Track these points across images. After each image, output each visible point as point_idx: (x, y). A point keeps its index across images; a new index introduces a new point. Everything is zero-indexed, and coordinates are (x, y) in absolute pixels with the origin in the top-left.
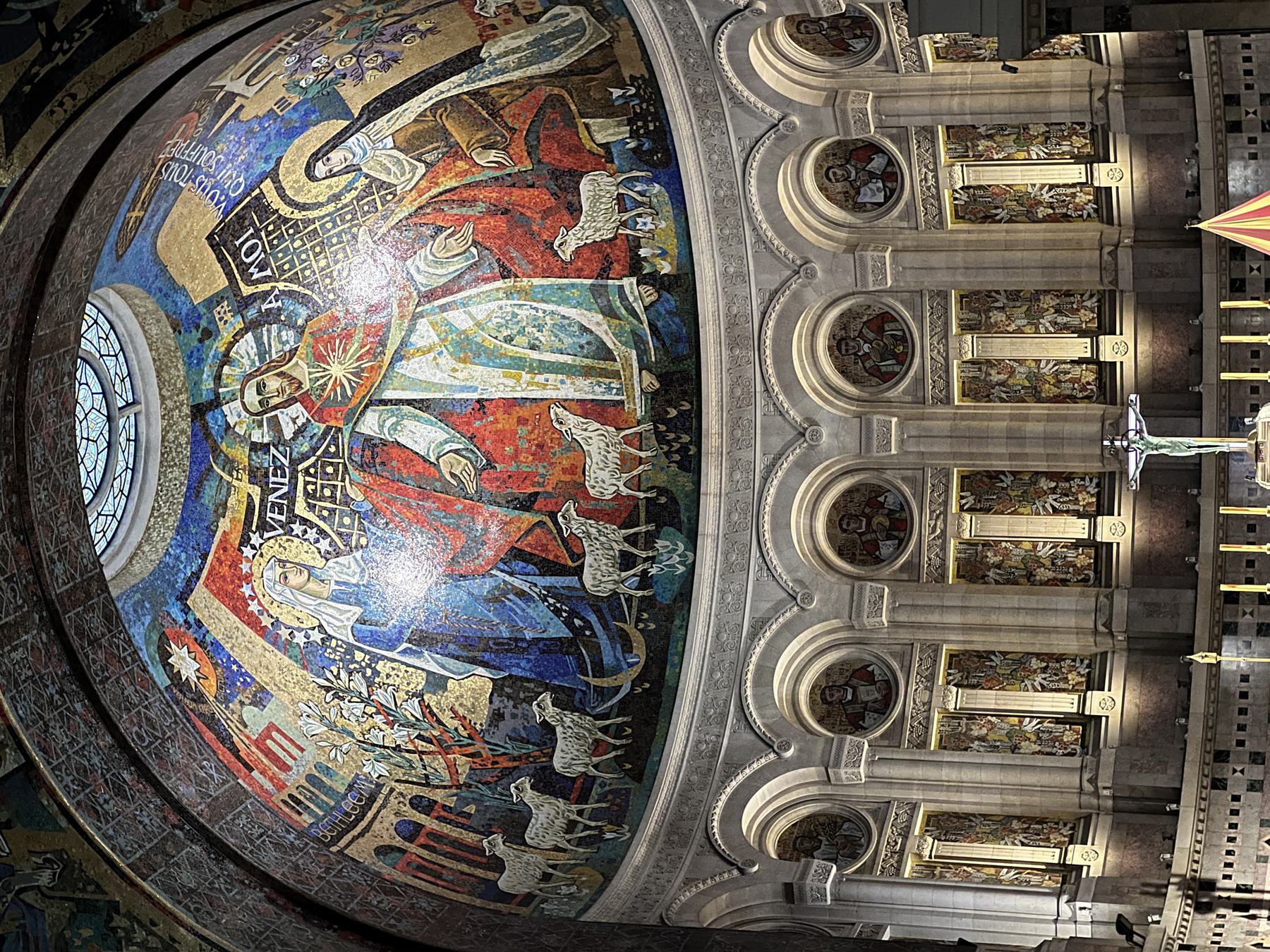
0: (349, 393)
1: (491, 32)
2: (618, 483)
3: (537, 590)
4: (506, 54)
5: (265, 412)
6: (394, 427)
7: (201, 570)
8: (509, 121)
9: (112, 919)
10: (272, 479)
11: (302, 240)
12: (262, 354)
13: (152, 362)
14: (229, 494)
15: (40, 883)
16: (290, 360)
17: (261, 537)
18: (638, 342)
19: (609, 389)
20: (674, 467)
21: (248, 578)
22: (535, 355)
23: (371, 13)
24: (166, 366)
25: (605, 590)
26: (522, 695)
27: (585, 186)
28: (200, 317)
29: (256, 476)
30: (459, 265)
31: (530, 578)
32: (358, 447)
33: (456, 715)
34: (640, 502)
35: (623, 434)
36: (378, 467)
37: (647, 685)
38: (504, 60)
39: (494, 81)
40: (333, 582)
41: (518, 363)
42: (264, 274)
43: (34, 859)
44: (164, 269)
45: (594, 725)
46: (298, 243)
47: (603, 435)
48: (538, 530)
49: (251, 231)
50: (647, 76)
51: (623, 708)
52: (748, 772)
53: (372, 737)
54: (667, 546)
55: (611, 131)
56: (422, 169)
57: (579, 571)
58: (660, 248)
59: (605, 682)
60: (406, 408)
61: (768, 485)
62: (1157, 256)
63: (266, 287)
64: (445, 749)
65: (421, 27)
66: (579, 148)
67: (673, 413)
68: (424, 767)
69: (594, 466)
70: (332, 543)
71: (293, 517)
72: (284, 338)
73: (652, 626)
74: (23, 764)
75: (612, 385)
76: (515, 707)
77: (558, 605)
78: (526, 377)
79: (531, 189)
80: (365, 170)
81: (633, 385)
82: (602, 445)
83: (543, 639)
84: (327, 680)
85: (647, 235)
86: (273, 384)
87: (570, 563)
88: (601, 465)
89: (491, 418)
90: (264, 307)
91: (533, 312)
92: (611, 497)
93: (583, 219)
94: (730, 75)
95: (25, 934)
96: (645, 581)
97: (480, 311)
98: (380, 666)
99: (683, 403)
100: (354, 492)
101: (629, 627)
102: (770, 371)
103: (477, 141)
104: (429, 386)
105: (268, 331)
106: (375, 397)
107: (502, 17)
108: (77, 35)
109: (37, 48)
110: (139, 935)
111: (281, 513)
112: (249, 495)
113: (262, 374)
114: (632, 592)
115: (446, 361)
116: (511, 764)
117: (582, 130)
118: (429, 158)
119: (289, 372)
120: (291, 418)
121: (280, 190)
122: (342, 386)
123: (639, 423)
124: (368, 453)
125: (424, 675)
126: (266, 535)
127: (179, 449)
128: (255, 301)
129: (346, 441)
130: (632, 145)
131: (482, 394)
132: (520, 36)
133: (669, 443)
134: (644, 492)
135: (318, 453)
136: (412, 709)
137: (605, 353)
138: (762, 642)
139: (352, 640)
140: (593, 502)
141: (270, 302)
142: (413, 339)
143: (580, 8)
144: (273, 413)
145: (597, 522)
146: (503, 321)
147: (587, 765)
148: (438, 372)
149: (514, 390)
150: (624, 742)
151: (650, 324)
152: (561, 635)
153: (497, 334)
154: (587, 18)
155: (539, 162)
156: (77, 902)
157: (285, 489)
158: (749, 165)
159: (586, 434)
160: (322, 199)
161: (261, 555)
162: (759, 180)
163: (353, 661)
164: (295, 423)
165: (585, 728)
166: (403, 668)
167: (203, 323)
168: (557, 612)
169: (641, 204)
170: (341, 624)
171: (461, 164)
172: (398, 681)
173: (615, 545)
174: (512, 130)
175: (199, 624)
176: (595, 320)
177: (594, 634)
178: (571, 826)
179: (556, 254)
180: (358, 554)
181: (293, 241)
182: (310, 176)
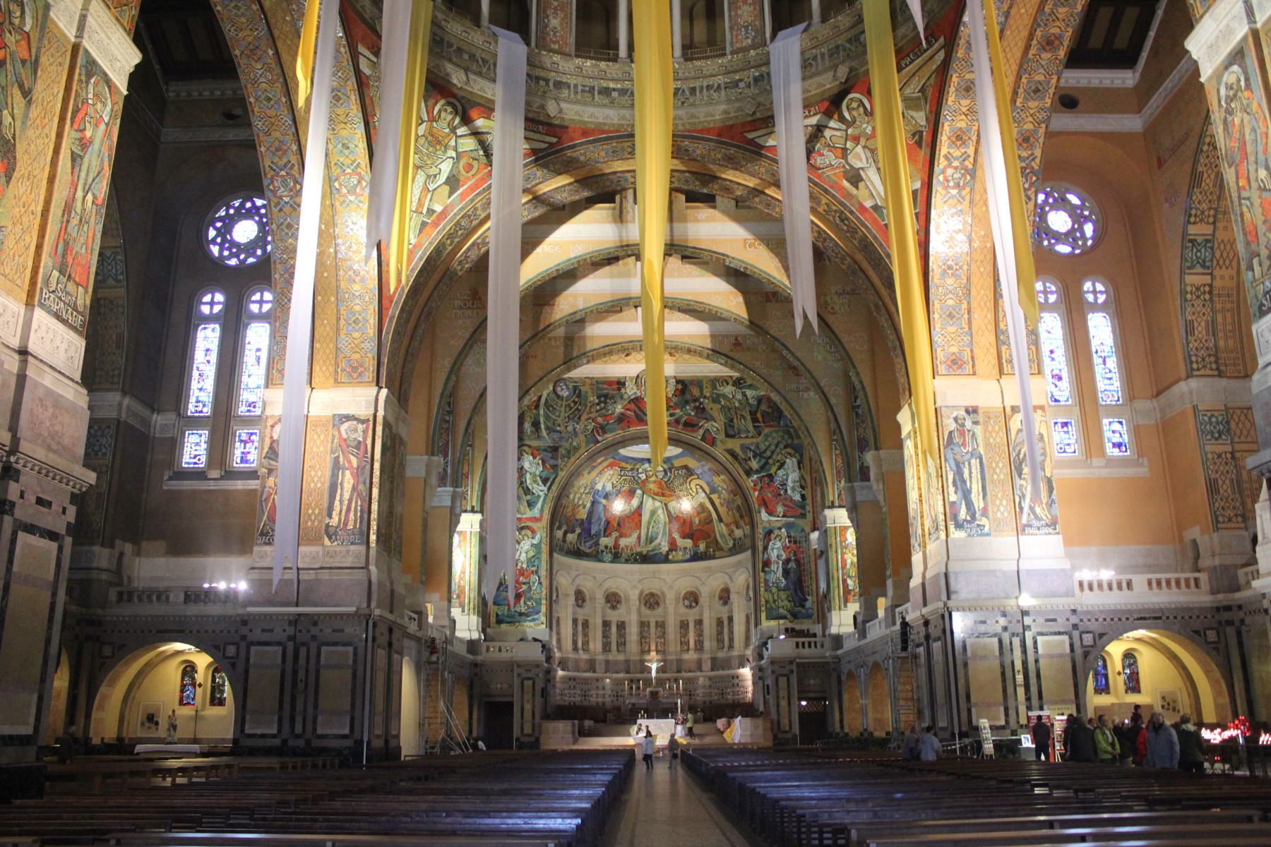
18: (653, 550)
27: (689, 541)
29: (632, 470)
41: (649, 523)
62: (675, 664)
66: (698, 540)
96: (602, 551)
97: (662, 516)
120: (643, 476)
137: (651, 542)
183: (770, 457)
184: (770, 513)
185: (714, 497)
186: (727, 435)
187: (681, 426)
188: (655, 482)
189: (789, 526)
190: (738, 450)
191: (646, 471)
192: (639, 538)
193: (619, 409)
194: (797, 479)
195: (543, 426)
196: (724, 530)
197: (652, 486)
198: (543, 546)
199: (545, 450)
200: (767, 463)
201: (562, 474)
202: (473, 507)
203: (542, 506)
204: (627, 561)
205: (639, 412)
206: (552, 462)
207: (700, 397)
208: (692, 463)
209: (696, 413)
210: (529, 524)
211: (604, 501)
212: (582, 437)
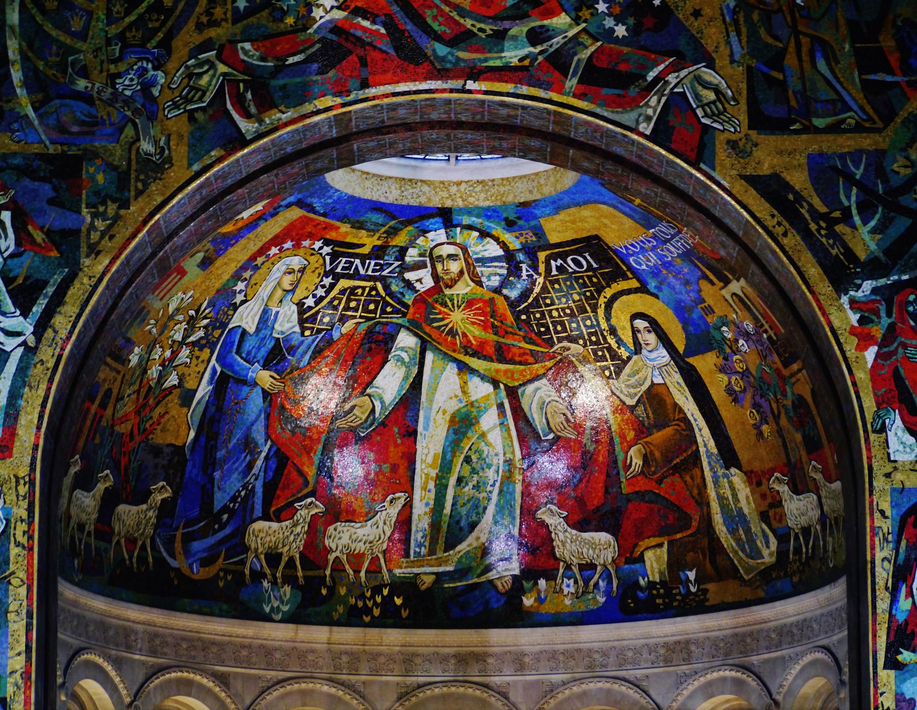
0: (435, 325)
1: (754, 481)
2: (338, 551)
3: (252, 481)
4: (732, 488)
5: (431, 259)
6: (400, 360)
7: (315, 212)
8: (668, 480)
9: (114, 201)
10: (373, 263)
11: (579, 301)
12: (483, 261)
13: (492, 178)
14: (368, 230)
15: (142, 142)
16: (472, 280)
17: (328, 254)
19: (420, 545)
20: (352, 601)
21: (297, 246)
22: (453, 481)
23: (784, 394)
24: (488, 191)
25: (251, 541)
26: (171, 471)
27: (604, 537)
28: (527, 220)
31: (262, 474)
33: (161, 416)
34: (322, 571)
35: (381, 556)
36: (367, 346)
37: (176, 583)
38: (727, 485)
40: (278, 309)
42: (554, 269)
43: (163, 139)
44: (578, 205)
45: (147, 537)
46: (576, 297)
47: (380, 538)
48: (301, 481)
49: (595, 266)
50: (707, 604)
52: (117, 680)
53: (158, 350)
54: (285, 595)
55: (655, 565)
56: (631, 402)
57: (266, 517)
58: (546, 598)
59: (178, 545)
60: (415, 370)
61: (339, 686)
63: (542, 268)
65: (765, 428)
67: (398, 601)
68: (129, 396)
69: (353, 530)
71: (337, 277)
72: (493, 278)
73: (221, 584)
74: (245, 138)
75: (423, 549)
76: (163, 466)
77: (239, 500)
78: (433, 473)
79: (603, 490)
80: (635, 357)
81: (423, 566)
82: (371, 538)
83: (213, 487)
84: (205, 309)
85: (558, 587)
87: (273, 509)
88: (354, 537)
89: (399, 441)
90: (524, 266)
91: (491, 482)
92: (327, 544)
93: (574, 532)
94: (708, 676)
95: (96, 124)
98: (207, 351)
99: (407, 611)
100: (349, 325)
102: (437, 690)
103: (651, 451)
104: (434, 389)
105: (502, 267)
106: (428, 346)
107: (768, 493)
108: (831, 241)
109: (823, 209)
110: (100, 224)
111: (343, 268)
112: (363, 245)
113: (465, 260)
114: (248, 566)
115: (453, 406)
116: (123, 467)
118: (640, 410)
119: (462, 279)
121: (629, 292)
122: (443, 319)
123: (390, 571)
124: (381, 337)
125: (195, 387)
126: (328, 258)
127: (415, 196)
128: (531, 260)
129: (394, 320)
130: (642, 582)
131: (421, 434)
132: (749, 503)
133: (373, 597)
134: (331, 575)
135: (387, 298)
137: (453, 540)
138: (211, 684)
139: (230, 326)
140: (322, 529)
141: (527, 271)
142: (476, 380)
143: (774, 559)
144: (429, 265)
145: (306, 533)
146: (484, 456)
147: (119, 534)
148: (444, 398)
149: (423, 461)
150: (135, 565)
152: (216, 503)
153: (473, 450)
154: (763, 563)
155: (629, 500)
156: (128, 172)
157: (362, 272)
158: (623, 683)
159: (381, 524)
160: (614, 321)
161: (312, 254)
162: (609, 691)
163: (214, 328)
164: (417, 281)
165: (145, 530)
166: (202, 371)
168: (233, 499)
169: (586, 582)
170: (244, 316)
171: (631, 435)
172: (193, 365)
173: (287, 548)
174: (660, 481)
175: (274, 215)
176: (482, 535)
177: (216, 532)
178: (81, 527)
180: (297, 329)
181: (579, 294)
182: (635, 316)
185: (705, 364)
187: (571, 83)
190: (799, 179)
191: (435, 260)
192: (404, 522)
195: (16, 75)
198: (14, 551)
199: (26, 171)
204: (353, 618)
206: (55, 218)
209: (633, 31)
211: (265, 378)
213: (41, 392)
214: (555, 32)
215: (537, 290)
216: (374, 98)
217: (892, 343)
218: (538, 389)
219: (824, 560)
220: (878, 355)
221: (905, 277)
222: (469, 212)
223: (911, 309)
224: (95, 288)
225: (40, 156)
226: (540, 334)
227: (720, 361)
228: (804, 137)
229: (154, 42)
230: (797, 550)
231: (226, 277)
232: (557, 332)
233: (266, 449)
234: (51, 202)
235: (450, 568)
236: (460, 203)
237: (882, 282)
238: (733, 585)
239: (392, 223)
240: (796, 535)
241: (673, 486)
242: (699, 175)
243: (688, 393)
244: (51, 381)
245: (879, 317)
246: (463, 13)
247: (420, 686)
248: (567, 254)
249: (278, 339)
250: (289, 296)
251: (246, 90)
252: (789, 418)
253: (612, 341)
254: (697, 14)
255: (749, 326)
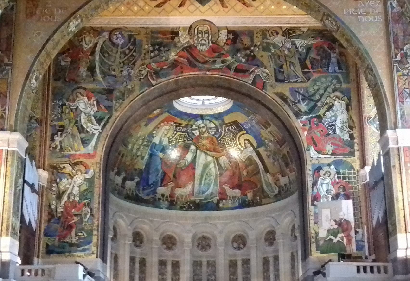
4: (268, 178)
6: (191, 152)
12: (210, 128)
18: (206, 199)
19: (196, 193)
21: (168, 123)
22: (204, 179)
27: (238, 191)
29: (186, 126)
30: (223, 166)
32: (188, 145)
33: (137, 162)
39: (262, 175)
41: (202, 176)
46: (232, 136)
49: (236, 128)
51: (137, 195)
56: (244, 160)
57: (161, 186)
59: (141, 191)
63: (224, 129)
64: (131, 160)
65: (275, 163)
66: (246, 190)
70: (171, 139)
71: (177, 132)
78: (199, 177)
80: (245, 150)
86: (204, 130)
90: (220, 129)
97: (213, 170)
101: (151, 196)
104: (199, 159)
115: (204, 162)
117: (250, 191)
120: (196, 133)
123: (190, 199)
126: (175, 127)
136: (139, 153)
139: (153, 142)
142: (209, 156)
151: (209, 202)
160: (240, 141)
163: (149, 142)
167: (219, 118)
168: (154, 182)
171: (244, 168)
174: (251, 177)
175: (162, 114)
178: (117, 184)
179: (224, 184)
180: (168, 144)
183: (319, 100)
184: (319, 152)
185: (261, 150)
186: (277, 80)
187: (232, 72)
188: (207, 138)
189: (337, 164)
191: (200, 128)
193: (173, 56)
194: (346, 120)
196: (269, 178)
197: (204, 142)
200: (315, 106)
201: (116, 114)
202: (11, 126)
203: (96, 144)
205: (192, 59)
206: (107, 103)
207: (252, 45)
208: (241, 118)
210: (81, 160)
212: (136, 81)
213: (103, 143)
214: (228, 61)
215: (222, 135)
216: (184, 76)
217: (311, 131)
218: (223, 158)
219: (290, 191)
220: (307, 133)
221: (314, 115)
222: (207, 115)
223: (315, 123)
224: (116, 119)
225: (104, 89)
226: (223, 145)
227: (265, 149)
228: (288, 84)
229: (131, 63)
230: (283, 190)
231: (151, 130)
232: (227, 145)
233: (161, 172)
234: (106, 99)
235: (203, 198)
236: (205, 114)
237: (308, 117)
238: (267, 200)
239: (189, 118)
240: (283, 187)
241: (253, 179)
242: (263, 93)
243: (257, 157)
244: (105, 140)
245: (307, 124)
246: (206, 57)
247: (196, 224)
248: (229, 125)
249: (164, 146)
250: (166, 136)
251: (153, 74)
252: (281, 160)
253: (240, 146)
254: (262, 56)
255: (272, 139)
